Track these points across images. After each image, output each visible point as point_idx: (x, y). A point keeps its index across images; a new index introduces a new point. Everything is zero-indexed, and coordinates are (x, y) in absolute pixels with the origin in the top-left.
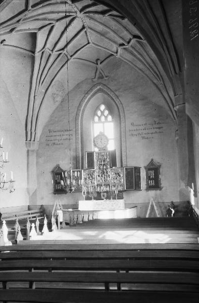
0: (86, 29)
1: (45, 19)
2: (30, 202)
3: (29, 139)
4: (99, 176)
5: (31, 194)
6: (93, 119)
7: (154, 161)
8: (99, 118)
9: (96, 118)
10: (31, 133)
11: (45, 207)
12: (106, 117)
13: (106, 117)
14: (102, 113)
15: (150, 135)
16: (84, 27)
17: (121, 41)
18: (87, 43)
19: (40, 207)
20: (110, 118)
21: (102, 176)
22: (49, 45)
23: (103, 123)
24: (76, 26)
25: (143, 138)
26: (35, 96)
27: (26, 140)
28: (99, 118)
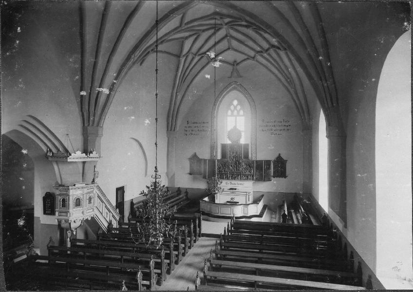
0: (228, 38)
1: (193, 30)
2: (169, 184)
3: (169, 129)
4: (231, 166)
5: (170, 177)
6: (227, 113)
7: (281, 156)
8: (232, 112)
9: (230, 112)
10: (172, 125)
11: (181, 189)
12: (238, 112)
13: (238, 112)
14: (235, 107)
15: (278, 132)
16: (226, 36)
17: (259, 49)
18: (227, 47)
19: (177, 189)
20: (242, 112)
21: (234, 166)
22: (194, 50)
23: (236, 116)
24: (221, 33)
25: (272, 134)
26: (176, 93)
27: (168, 130)
28: (232, 112)
